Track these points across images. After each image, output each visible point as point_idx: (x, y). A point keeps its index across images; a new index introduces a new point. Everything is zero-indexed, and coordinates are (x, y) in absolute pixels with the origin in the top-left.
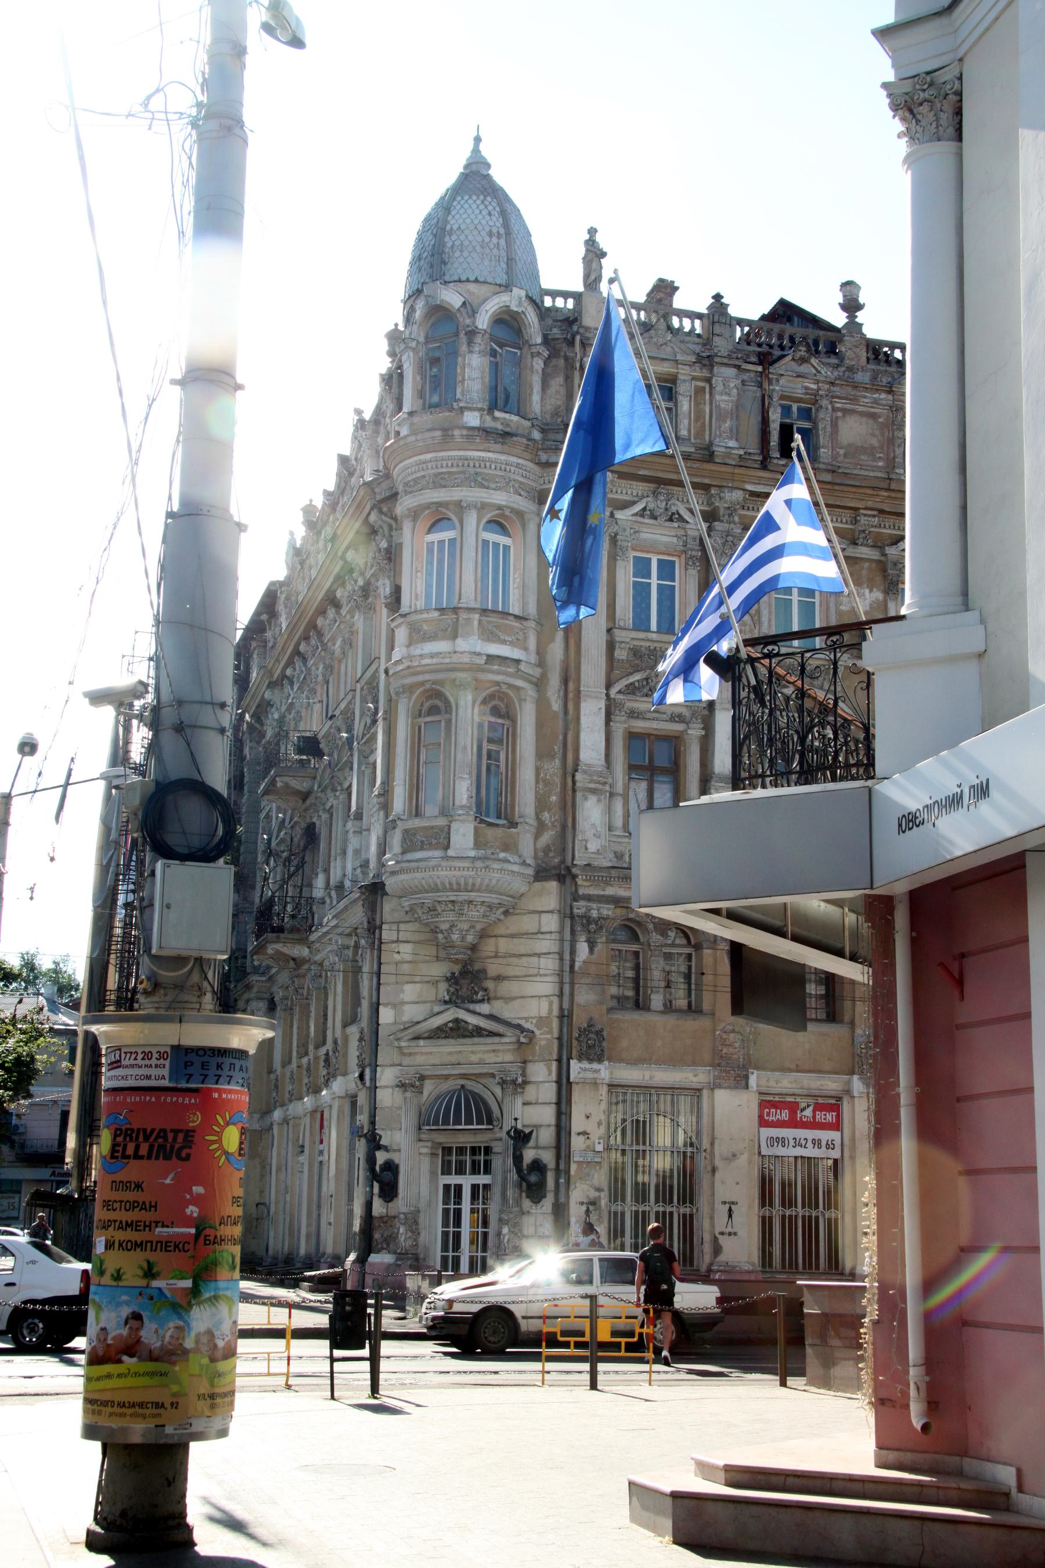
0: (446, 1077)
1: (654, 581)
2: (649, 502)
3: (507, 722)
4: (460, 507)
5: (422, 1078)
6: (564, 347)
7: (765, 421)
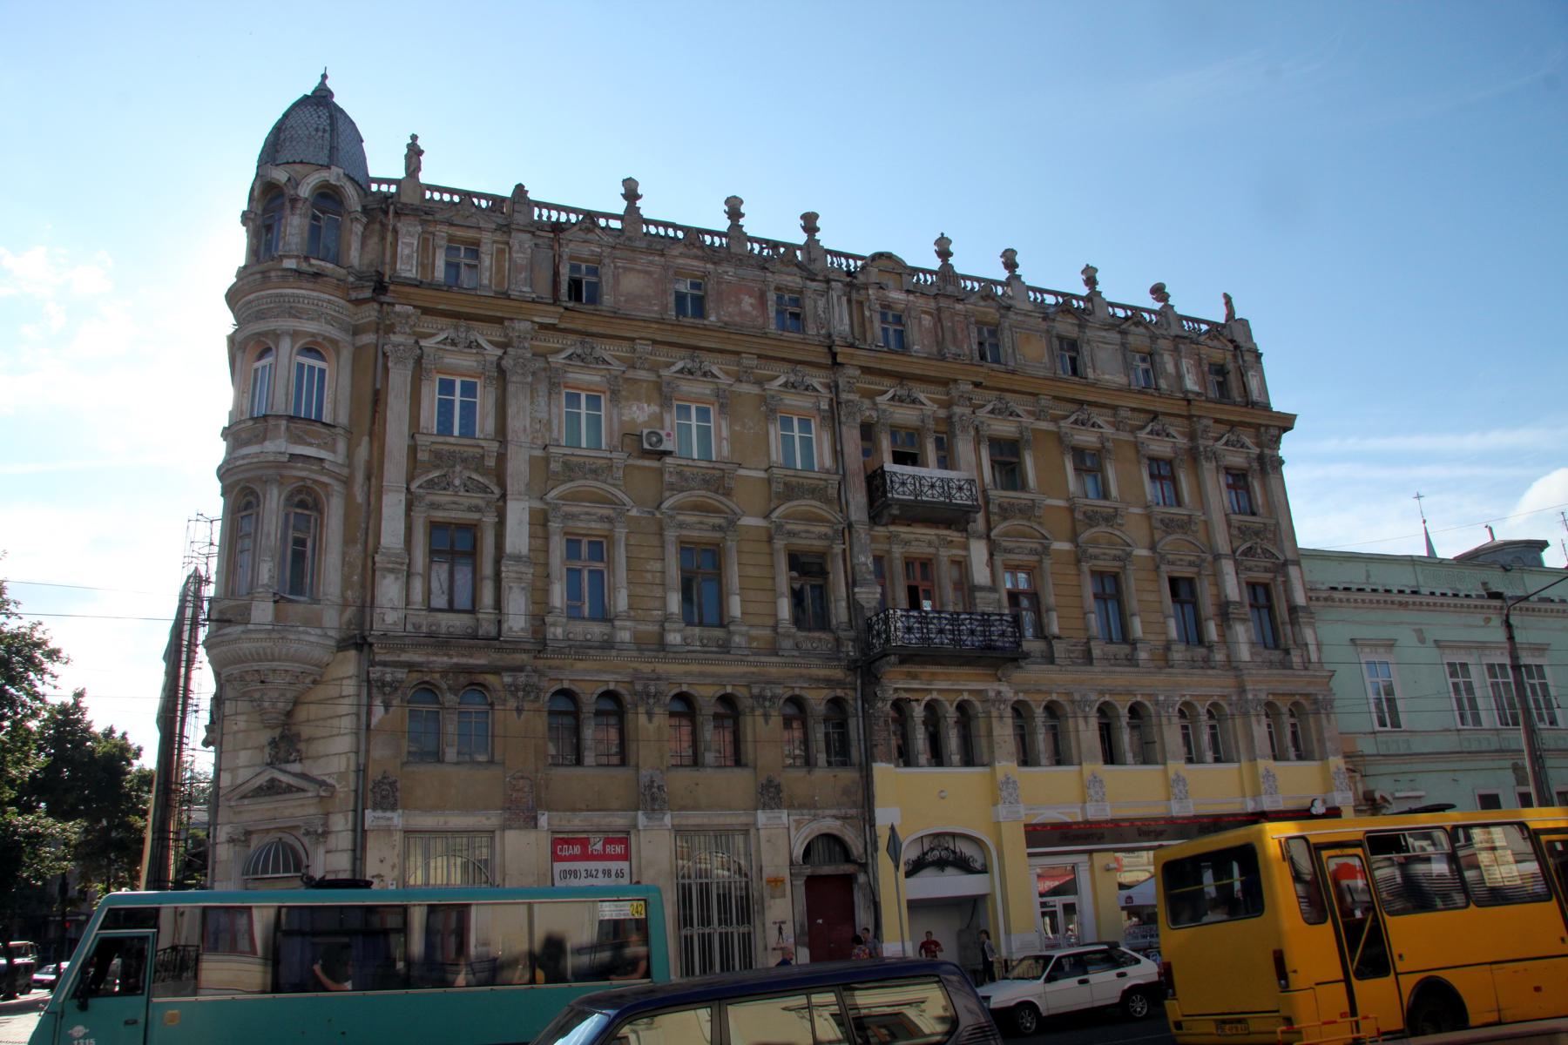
0: (268, 831)
1: (457, 398)
2: (451, 333)
3: (314, 514)
4: (276, 335)
5: (248, 833)
6: (381, 216)
7: (556, 274)
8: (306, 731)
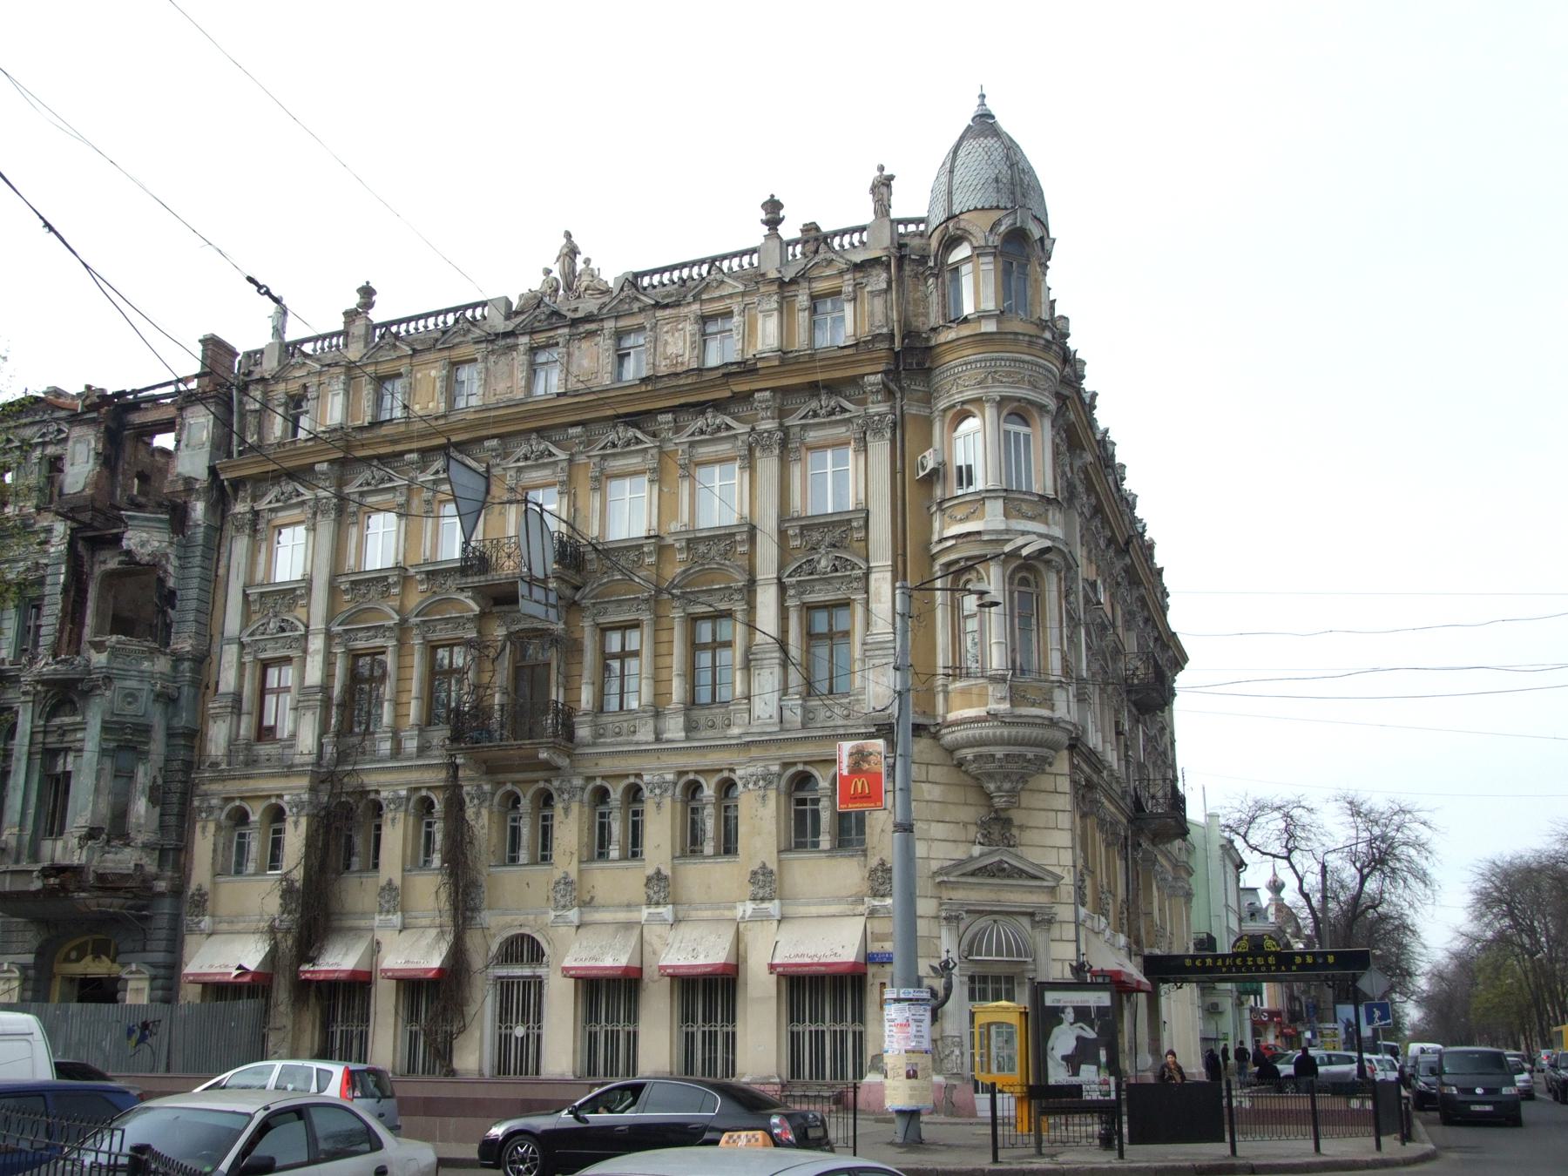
8: (1017, 816)
